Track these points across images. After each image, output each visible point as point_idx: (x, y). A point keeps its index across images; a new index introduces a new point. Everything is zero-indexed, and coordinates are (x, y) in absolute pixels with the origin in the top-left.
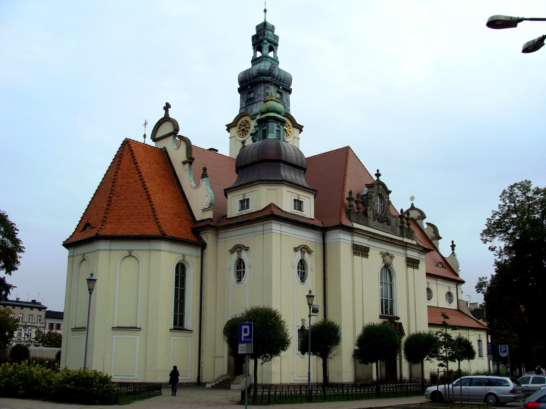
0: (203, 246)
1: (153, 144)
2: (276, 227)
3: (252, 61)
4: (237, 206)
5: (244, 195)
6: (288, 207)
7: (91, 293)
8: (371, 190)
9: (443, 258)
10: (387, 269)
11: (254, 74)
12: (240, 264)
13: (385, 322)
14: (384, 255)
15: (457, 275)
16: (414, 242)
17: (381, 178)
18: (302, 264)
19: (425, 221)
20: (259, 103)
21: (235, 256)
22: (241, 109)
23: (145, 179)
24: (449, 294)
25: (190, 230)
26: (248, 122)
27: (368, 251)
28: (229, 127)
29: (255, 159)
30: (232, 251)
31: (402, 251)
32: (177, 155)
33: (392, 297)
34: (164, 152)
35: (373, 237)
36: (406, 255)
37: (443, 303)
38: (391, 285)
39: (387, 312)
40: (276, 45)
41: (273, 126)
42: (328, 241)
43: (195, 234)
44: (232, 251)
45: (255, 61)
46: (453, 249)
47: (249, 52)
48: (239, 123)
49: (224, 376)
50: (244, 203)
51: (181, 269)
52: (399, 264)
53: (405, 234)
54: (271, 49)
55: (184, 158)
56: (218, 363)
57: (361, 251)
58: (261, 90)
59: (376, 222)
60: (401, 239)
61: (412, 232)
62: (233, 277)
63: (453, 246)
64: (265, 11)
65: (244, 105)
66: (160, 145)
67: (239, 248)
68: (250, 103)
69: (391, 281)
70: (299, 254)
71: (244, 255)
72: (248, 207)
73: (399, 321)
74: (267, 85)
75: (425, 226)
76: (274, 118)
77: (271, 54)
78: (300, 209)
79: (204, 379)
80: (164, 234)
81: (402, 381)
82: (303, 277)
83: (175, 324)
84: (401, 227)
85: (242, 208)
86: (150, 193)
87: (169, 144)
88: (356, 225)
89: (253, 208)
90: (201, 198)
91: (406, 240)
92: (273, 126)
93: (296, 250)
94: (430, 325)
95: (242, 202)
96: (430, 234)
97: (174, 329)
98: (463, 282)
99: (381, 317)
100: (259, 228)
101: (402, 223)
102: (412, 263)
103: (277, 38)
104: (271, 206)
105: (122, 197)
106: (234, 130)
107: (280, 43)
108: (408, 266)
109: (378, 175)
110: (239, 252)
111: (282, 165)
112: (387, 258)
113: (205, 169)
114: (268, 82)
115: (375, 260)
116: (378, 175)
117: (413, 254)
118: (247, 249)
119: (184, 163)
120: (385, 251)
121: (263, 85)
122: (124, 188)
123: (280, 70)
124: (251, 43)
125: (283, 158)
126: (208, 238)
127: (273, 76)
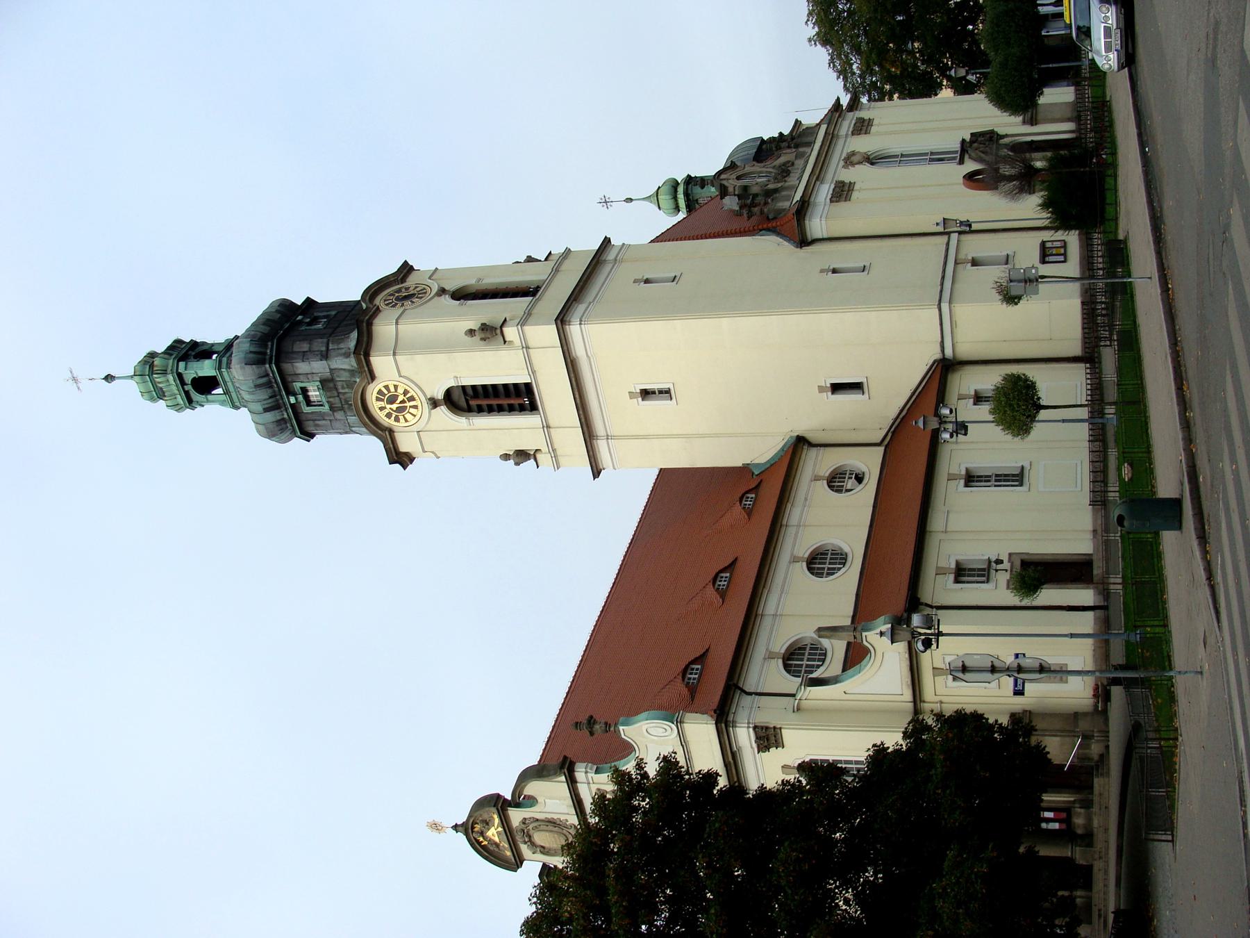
13: (970, 157)
14: (849, 161)
16: (824, 127)
27: (843, 182)
31: (841, 142)
33: (926, 154)
35: (818, 175)
38: (902, 155)
39: (949, 159)
52: (862, 144)
57: (842, 192)
69: (896, 156)
73: (968, 138)
81: (1078, 130)
115: (859, 175)
120: (842, 163)
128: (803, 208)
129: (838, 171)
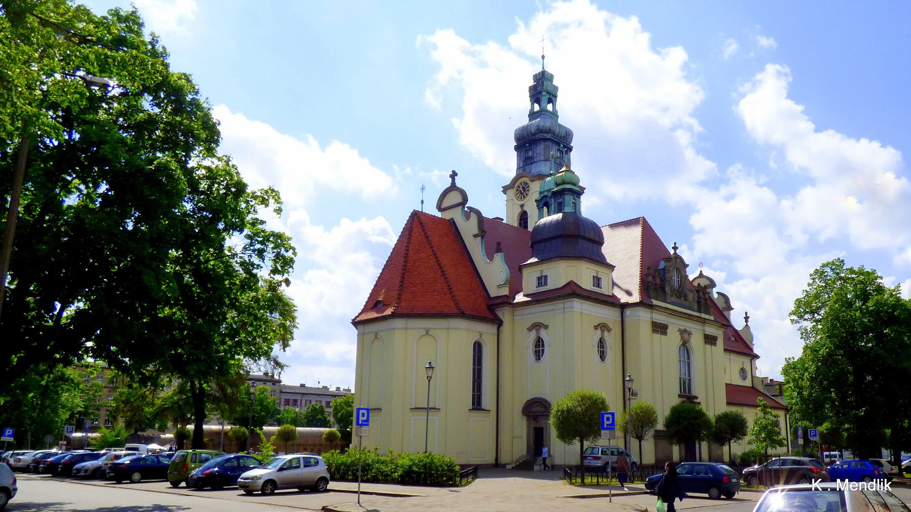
0: (499, 323)
1: (439, 214)
2: (577, 305)
3: (529, 116)
4: (535, 282)
6: (587, 284)
7: (429, 378)
8: (668, 264)
9: (736, 330)
10: (685, 347)
11: (533, 131)
12: (539, 344)
13: (684, 402)
14: (683, 332)
15: (751, 350)
16: (712, 318)
17: (678, 251)
18: (601, 343)
19: (715, 290)
20: (538, 164)
21: (534, 333)
22: (518, 168)
23: (438, 254)
24: (743, 370)
25: (485, 307)
28: (505, 189)
29: (552, 235)
30: (530, 329)
32: (468, 229)
33: (689, 375)
34: (452, 223)
35: (673, 313)
36: (704, 331)
37: (737, 381)
38: (689, 363)
39: (685, 390)
40: (556, 97)
41: (569, 198)
42: (626, 319)
43: (489, 310)
44: (530, 329)
45: (532, 115)
46: (747, 321)
47: (524, 104)
48: (517, 185)
49: (522, 457)
50: (542, 280)
51: (478, 348)
52: (696, 341)
53: (702, 309)
54: (550, 101)
55: (476, 231)
56: (516, 444)
57: (660, 329)
58: (540, 148)
59: (674, 299)
60: (698, 314)
61: (705, 303)
62: (531, 356)
63: (747, 318)
65: (521, 165)
66: (448, 215)
67: (537, 326)
68: (528, 162)
69: (689, 359)
70: (599, 332)
71: (543, 334)
72: (546, 284)
73: (698, 401)
74: (547, 143)
75: (716, 296)
76: (570, 190)
77: (550, 107)
78: (598, 286)
79: (505, 458)
80: (463, 313)
82: (602, 356)
83: (473, 404)
84: (699, 303)
85: (539, 285)
86: (445, 269)
87: (456, 215)
88: (655, 302)
89: (552, 284)
90: (494, 273)
91: (703, 315)
92: (569, 198)
93: (596, 328)
94: (728, 403)
95: (539, 279)
96: (721, 304)
97: (473, 409)
98: (757, 357)
99: (680, 396)
100: (559, 305)
101: (699, 298)
102: (710, 340)
103: (556, 88)
104: (571, 284)
105: (415, 273)
106: (512, 192)
107: (559, 94)
108: (706, 343)
109: (675, 248)
110: (538, 331)
111: (580, 241)
112: (686, 336)
113: (499, 244)
114: (549, 139)
115: (673, 337)
116: (675, 248)
117: (711, 330)
118: (546, 327)
119: (475, 236)
120: (683, 328)
121: (542, 141)
122: (417, 264)
123: (560, 126)
124: (528, 94)
125: (582, 234)
126: (504, 314)
127: (554, 133)
128: (651, 307)
129: (675, 325)
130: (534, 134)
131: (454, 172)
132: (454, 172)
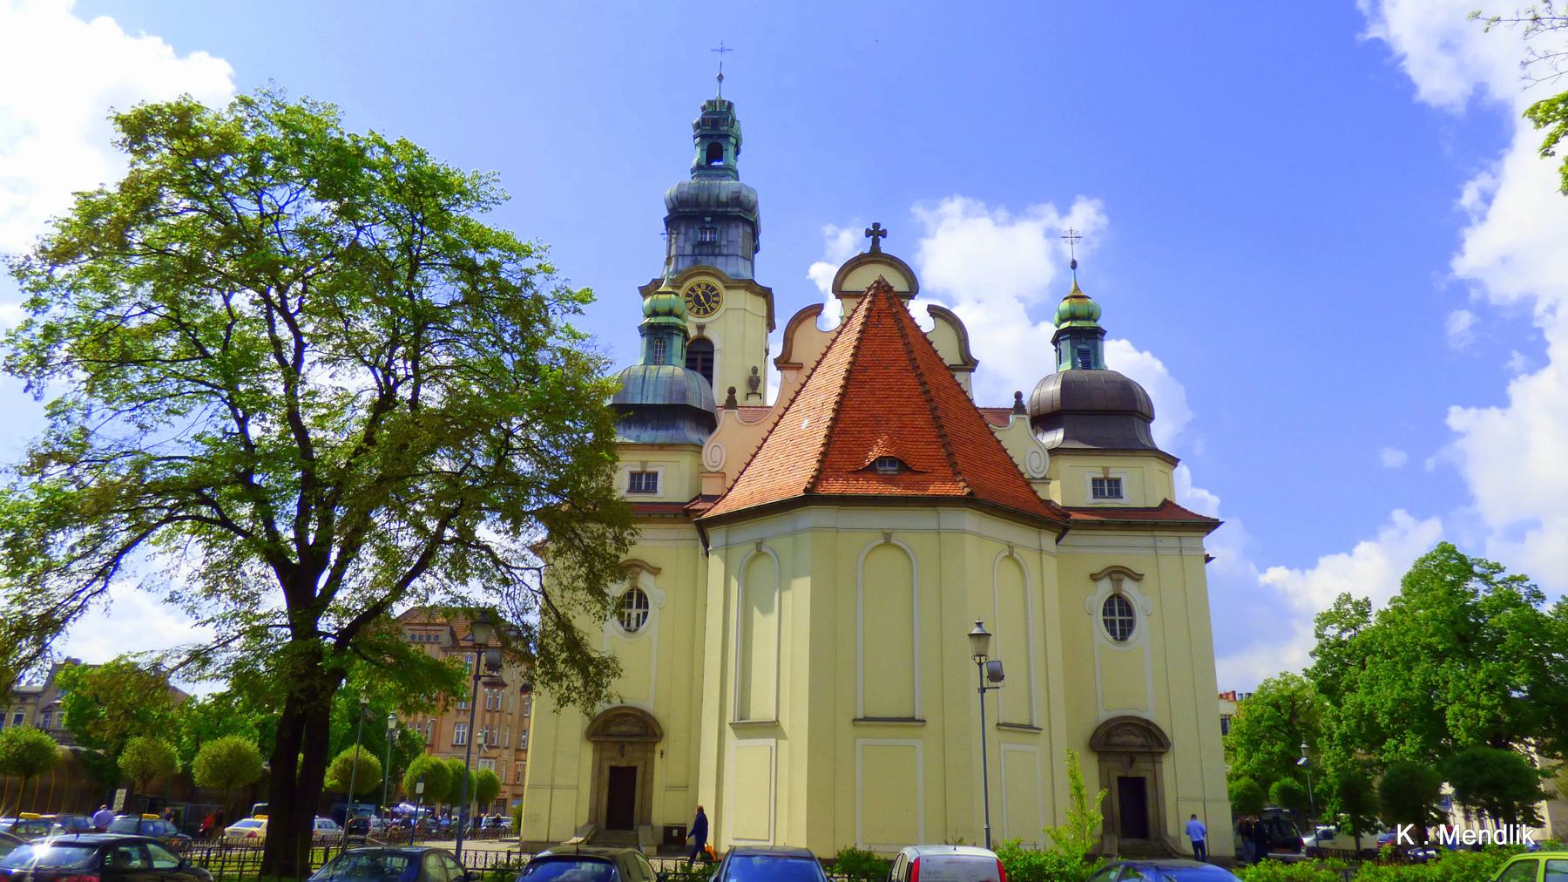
5: (1106, 469)
11: (723, 198)
26: (713, 289)
30: (1095, 578)
44: (1095, 578)
64: (720, 78)
67: (1117, 573)
68: (705, 251)
71: (1129, 589)
110: (1117, 582)
118: (1137, 578)
130: (719, 204)
131: (876, 226)
132: (876, 226)
